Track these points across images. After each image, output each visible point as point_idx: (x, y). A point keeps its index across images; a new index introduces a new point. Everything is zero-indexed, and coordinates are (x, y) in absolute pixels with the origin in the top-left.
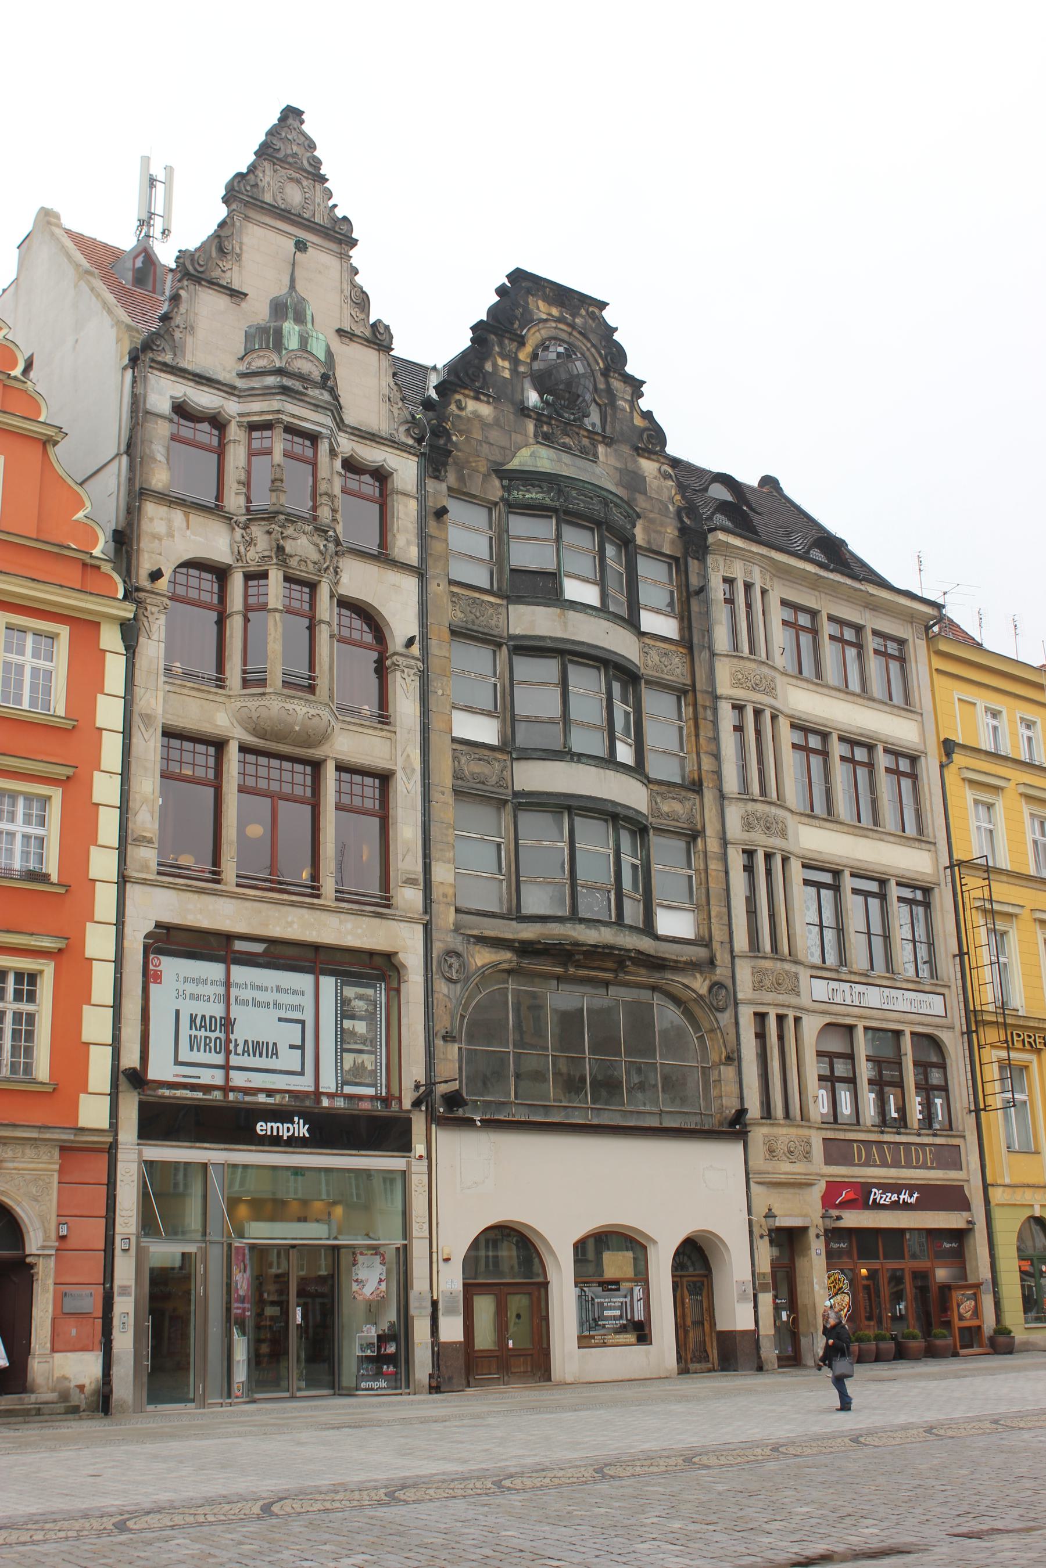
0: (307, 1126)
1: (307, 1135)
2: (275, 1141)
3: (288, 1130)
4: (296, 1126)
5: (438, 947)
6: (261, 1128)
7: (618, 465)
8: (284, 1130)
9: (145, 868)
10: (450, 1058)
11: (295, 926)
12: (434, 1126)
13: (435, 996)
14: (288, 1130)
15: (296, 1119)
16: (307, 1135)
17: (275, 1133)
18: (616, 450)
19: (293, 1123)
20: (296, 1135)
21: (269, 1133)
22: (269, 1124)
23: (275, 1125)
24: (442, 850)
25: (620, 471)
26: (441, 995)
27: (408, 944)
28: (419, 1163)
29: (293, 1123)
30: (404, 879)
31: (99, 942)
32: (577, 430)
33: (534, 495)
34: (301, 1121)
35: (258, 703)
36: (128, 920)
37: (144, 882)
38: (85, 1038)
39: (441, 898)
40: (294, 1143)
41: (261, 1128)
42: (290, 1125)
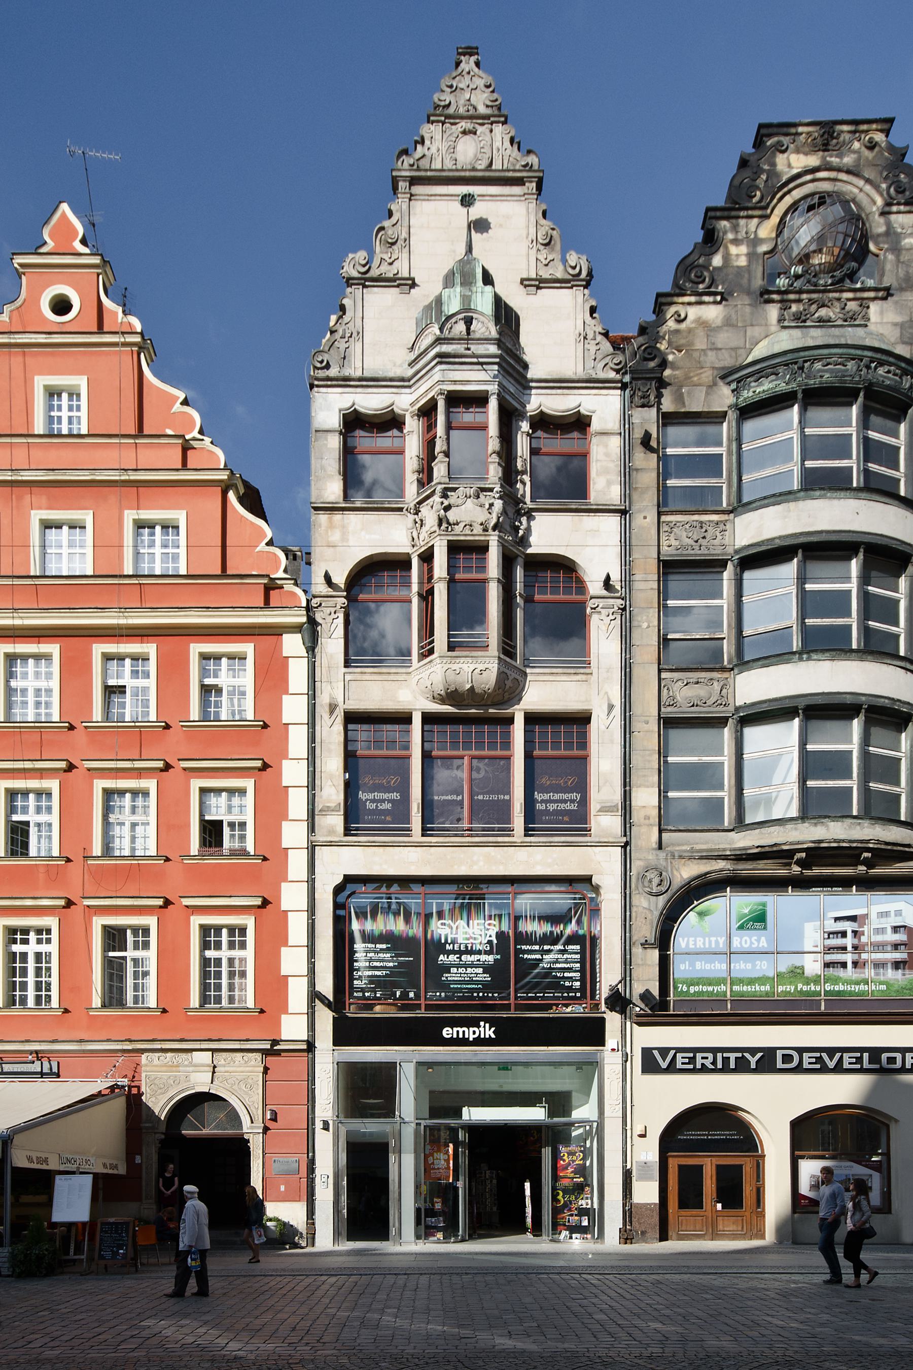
0: (493, 1029)
1: (493, 1036)
2: (463, 1042)
3: (474, 1032)
4: (482, 1029)
5: (637, 866)
6: (447, 1032)
7: (899, 319)
8: (470, 1033)
9: (331, 831)
10: (649, 963)
11: (481, 863)
12: (628, 1023)
13: (634, 909)
14: (474, 1032)
15: (482, 1023)
16: (493, 1036)
17: (461, 1036)
18: (896, 302)
19: (479, 1027)
20: (482, 1036)
21: (455, 1036)
22: (455, 1029)
23: (461, 1030)
24: (644, 776)
25: (902, 326)
26: (640, 909)
27: (605, 867)
28: (615, 1053)
29: (479, 1027)
30: (598, 807)
31: (292, 897)
32: (836, 295)
33: (765, 388)
34: (487, 1025)
35: (428, 672)
36: (318, 876)
37: (330, 844)
38: (283, 972)
39: (642, 820)
40: (479, 1042)
41: (447, 1032)
42: (475, 1029)
